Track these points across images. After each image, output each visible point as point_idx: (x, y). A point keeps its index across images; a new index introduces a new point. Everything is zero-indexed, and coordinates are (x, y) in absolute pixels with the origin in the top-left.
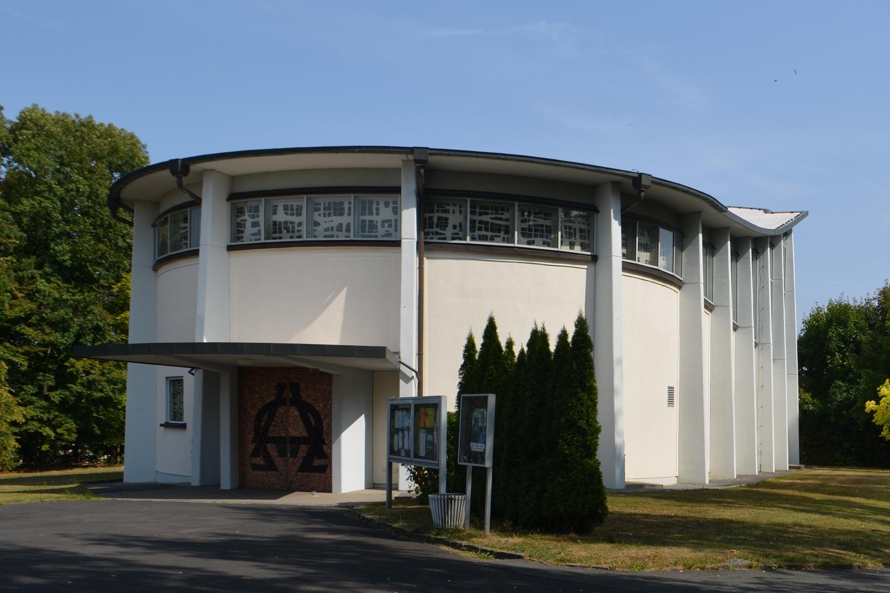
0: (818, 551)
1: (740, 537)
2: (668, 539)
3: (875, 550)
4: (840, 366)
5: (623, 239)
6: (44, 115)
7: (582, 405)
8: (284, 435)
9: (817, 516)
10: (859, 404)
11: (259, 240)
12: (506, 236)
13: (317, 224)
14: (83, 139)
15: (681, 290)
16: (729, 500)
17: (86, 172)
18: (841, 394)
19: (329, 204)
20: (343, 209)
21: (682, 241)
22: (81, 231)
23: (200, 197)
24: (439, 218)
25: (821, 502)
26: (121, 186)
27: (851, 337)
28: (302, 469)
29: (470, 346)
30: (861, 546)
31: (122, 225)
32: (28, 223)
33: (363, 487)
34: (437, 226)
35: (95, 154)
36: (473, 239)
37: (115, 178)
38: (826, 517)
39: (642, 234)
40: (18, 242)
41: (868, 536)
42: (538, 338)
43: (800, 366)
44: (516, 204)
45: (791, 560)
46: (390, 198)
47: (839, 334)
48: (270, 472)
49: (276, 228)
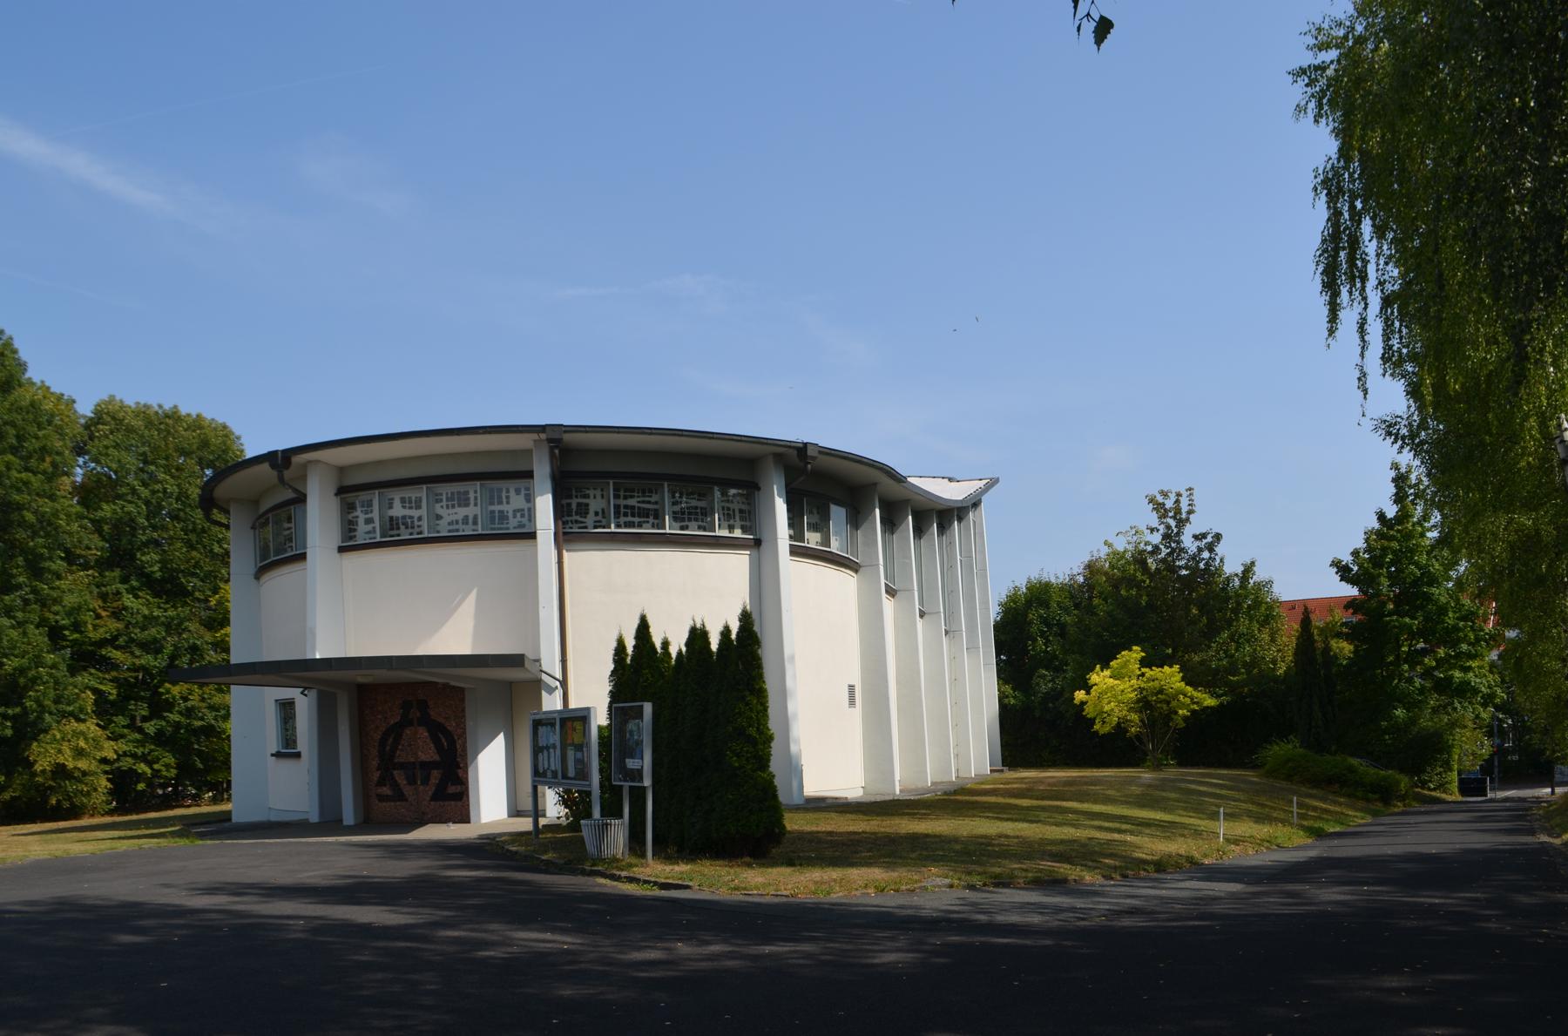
0: (1027, 864)
1: (937, 853)
2: (857, 858)
3: (1093, 861)
4: (1043, 652)
5: (789, 519)
6: (122, 407)
7: (751, 710)
8: (412, 760)
9: (1025, 825)
10: (1067, 695)
11: (375, 538)
12: (656, 521)
13: (439, 517)
14: (169, 433)
15: (859, 573)
16: (924, 811)
17: (173, 471)
18: (1046, 685)
19: (452, 494)
20: (468, 499)
21: (856, 519)
22: (171, 538)
23: (303, 491)
24: (579, 505)
25: (1028, 808)
26: (213, 484)
27: (1054, 618)
28: (435, 798)
29: (620, 648)
30: (1076, 857)
31: (218, 529)
32: (109, 531)
33: (505, 816)
34: (577, 514)
35: (182, 448)
36: (618, 526)
37: (207, 476)
38: (1035, 825)
39: (811, 512)
40: (99, 553)
41: (1084, 845)
42: (698, 636)
43: (998, 655)
44: (611, 482)
45: (997, 876)
46: (521, 483)
47: (1041, 616)
48: (398, 803)
49: (393, 524)
